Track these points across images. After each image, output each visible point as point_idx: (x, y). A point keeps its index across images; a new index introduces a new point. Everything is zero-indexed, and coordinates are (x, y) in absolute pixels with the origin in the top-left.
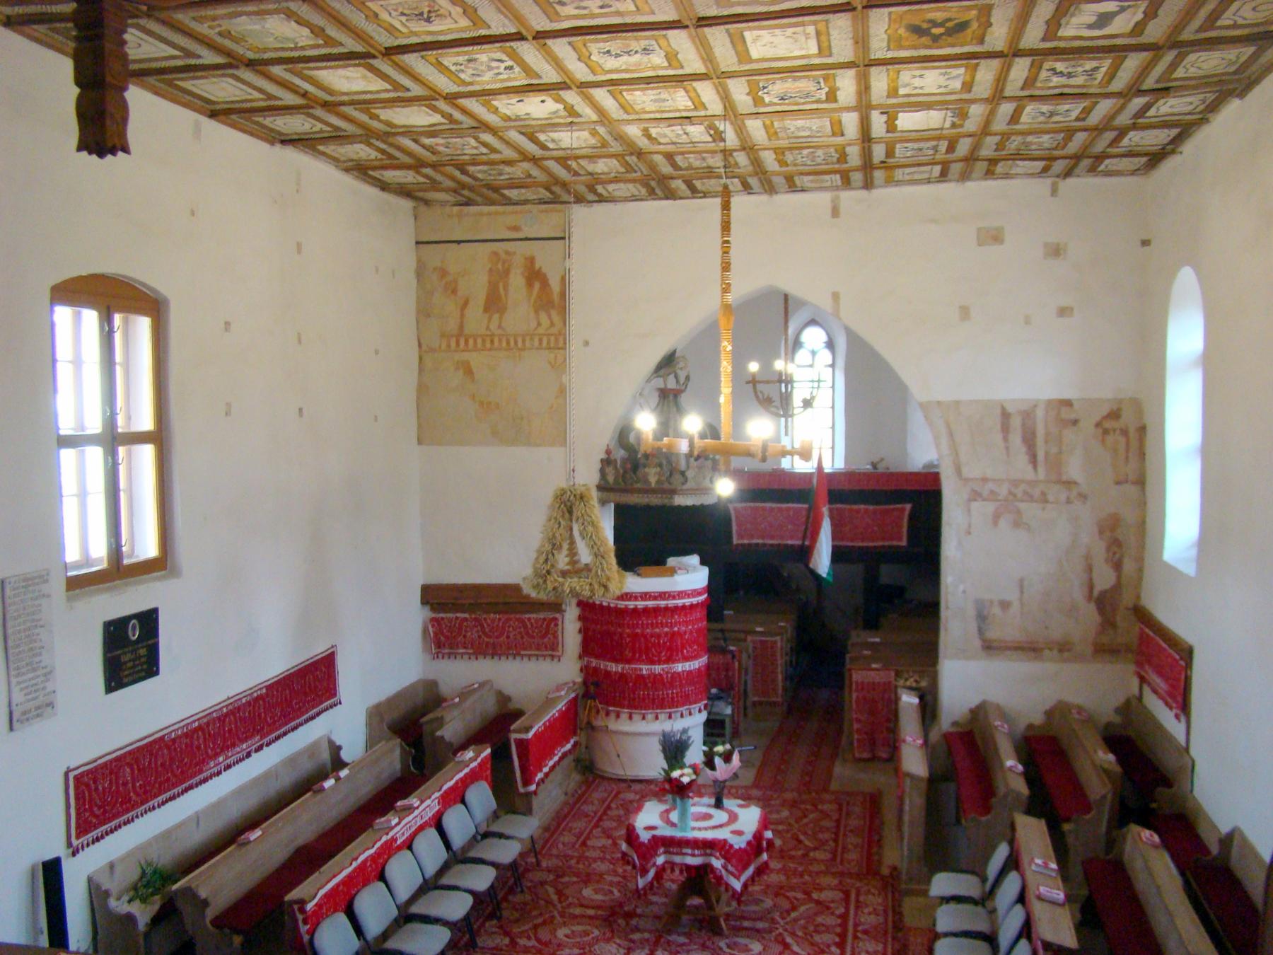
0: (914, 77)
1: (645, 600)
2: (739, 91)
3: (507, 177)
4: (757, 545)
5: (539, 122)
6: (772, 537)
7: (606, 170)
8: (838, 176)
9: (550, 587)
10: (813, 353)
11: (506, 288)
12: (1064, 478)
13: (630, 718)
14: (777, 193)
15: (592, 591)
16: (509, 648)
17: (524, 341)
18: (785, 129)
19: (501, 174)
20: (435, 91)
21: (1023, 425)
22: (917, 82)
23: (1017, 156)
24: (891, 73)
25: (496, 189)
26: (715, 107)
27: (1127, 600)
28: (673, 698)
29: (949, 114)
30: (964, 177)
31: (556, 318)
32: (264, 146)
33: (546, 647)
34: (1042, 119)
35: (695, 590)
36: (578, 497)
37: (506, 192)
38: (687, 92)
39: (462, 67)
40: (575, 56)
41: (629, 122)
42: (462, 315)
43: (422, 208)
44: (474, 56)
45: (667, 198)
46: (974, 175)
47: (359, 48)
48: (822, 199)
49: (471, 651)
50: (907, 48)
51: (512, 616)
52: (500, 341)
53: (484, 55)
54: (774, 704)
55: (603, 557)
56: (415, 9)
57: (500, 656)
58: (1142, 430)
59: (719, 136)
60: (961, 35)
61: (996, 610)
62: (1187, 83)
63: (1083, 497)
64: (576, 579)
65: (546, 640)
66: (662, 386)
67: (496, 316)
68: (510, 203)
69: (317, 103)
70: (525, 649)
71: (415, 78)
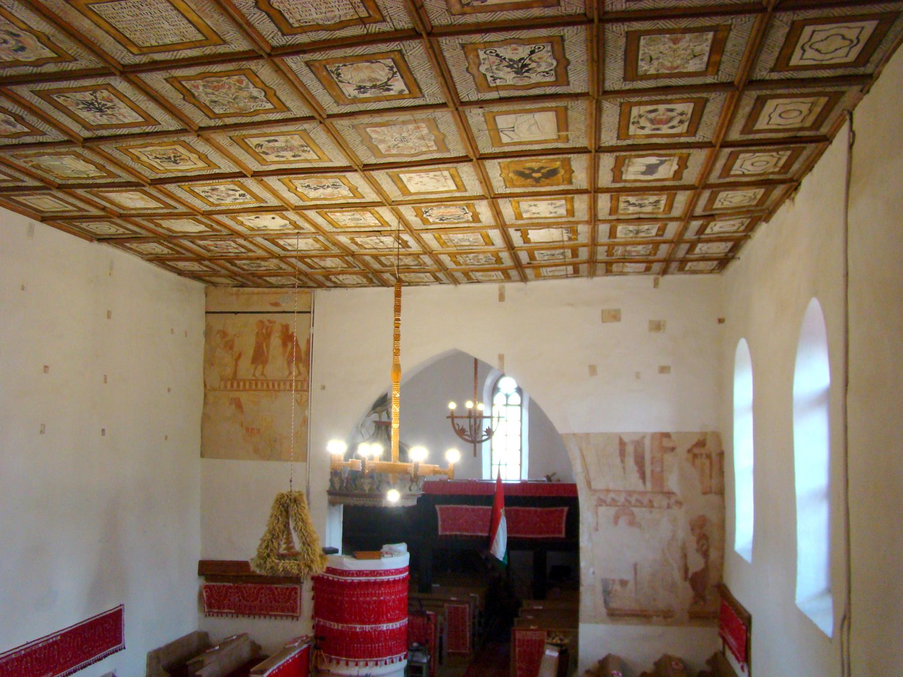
0: (531, 206)
2: (408, 213)
3: (264, 268)
4: (456, 535)
5: (276, 232)
6: (467, 530)
7: (334, 266)
8: (500, 273)
9: (268, 566)
10: (507, 396)
11: (268, 346)
12: (665, 489)
13: (347, 664)
14: (460, 283)
15: (299, 570)
16: (261, 610)
17: (279, 385)
18: (452, 241)
19: (260, 267)
20: (193, 209)
21: (636, 450)
22: (534, 209)
23: (624, 260)
24: (514, 204)
25: (260, 277)
26: (394, 223)
27: (712, 580)
28: (379, 650)
29: (564, 231)
30: (592, 274)
31: (302, 369)
32: (86, 243)
33: (288, 610)
34: (631, 235)
35: (397, 570)
36: (293, 500)
37: (267, 279)
38: (372, 214)
39: (209, 194)
40: (286, 188)
41: (338, 233)
42: (236, 365)
43: (212, 288)
44: (218, 187)
45: (383, 286)
46: (599, 272)
47: (132, 179)
48: (491, 289)
49: (233, 611)
50: (519, 187)
51: (264, 586)
52: (262, 385)
53: (223, 187)
54: (463, 655)
55: (309, 545)
56: (165, 154)
57: (254, 615)
58: (721, 454)
59: (405, 245)
60: (554, 178)
61: (617, 587)
62: (725, 211)
63: (679, 503)
64: (287, 561)
65: (289, 604)
66: (378, 419)
67: (260, 367)
68: (272, 286)
69: (114, 215)
70: (272, 611)
71: (177, 200)
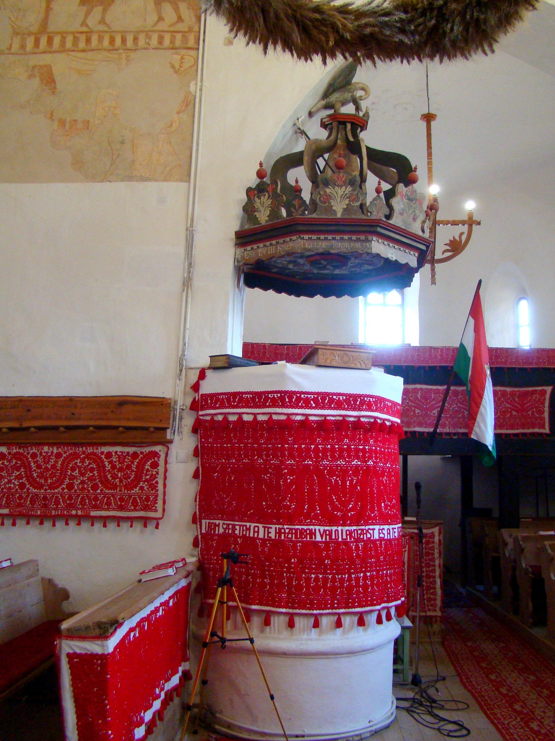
1: (323, 408)
16: (71, 506)
17: (136, 39)
28: (365, 587)
52: (101, 39)
57: (54, 519)
67: (97, 11)
70: (97, 507)
